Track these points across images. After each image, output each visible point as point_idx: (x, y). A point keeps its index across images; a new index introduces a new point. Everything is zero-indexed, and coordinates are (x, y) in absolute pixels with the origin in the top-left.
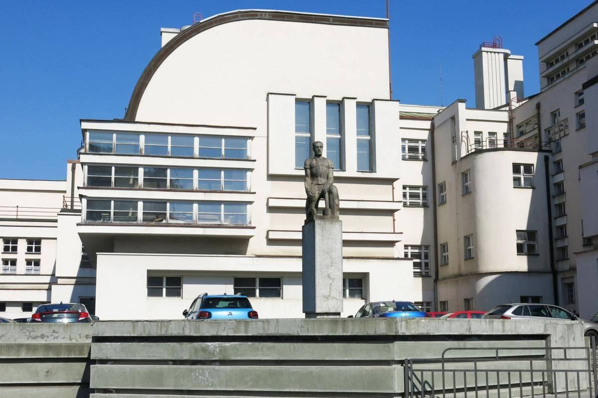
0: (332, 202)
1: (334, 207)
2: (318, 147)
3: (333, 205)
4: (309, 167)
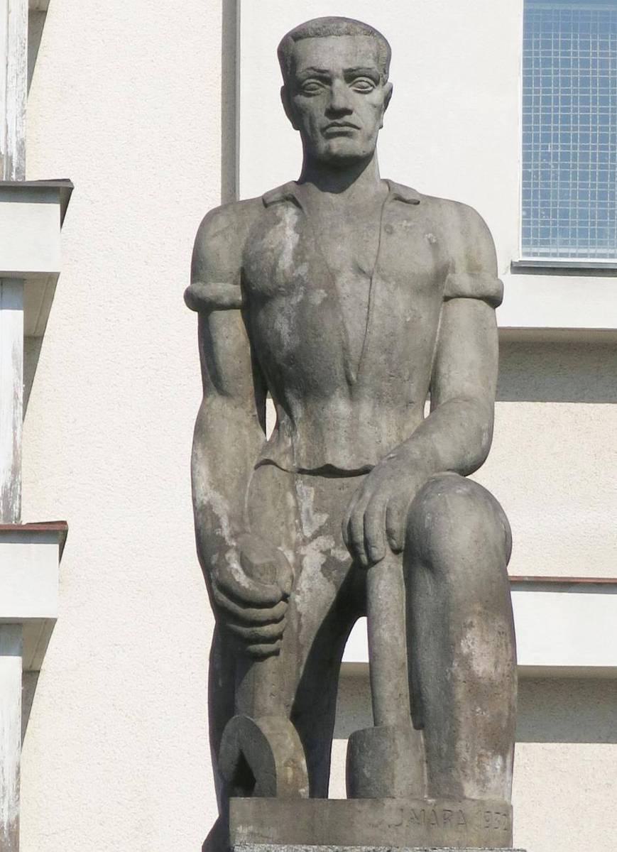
0: (429, 658)
1: (450, 709)
2: (325, 78)
3: (447, 688)
4: (229, 290)
